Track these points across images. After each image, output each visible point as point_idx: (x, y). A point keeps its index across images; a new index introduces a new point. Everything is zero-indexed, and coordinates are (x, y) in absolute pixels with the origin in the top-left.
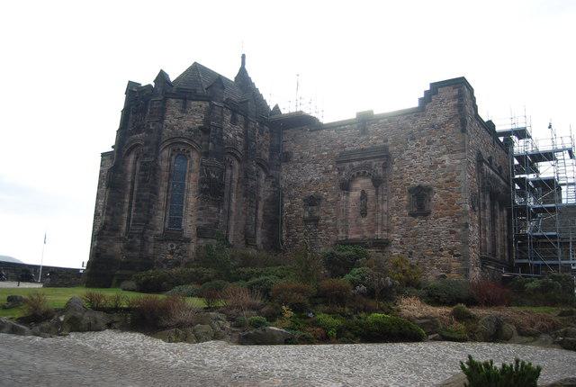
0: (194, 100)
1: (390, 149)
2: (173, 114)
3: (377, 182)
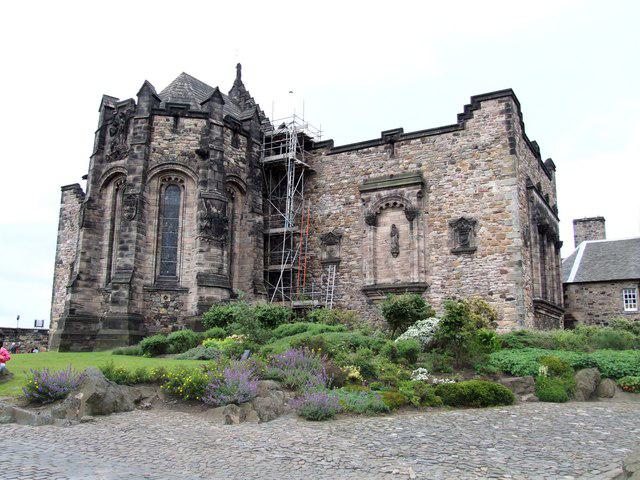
0: (187, 117)
1: (425, 175)
2: (162, 134)
3: (411, 215)
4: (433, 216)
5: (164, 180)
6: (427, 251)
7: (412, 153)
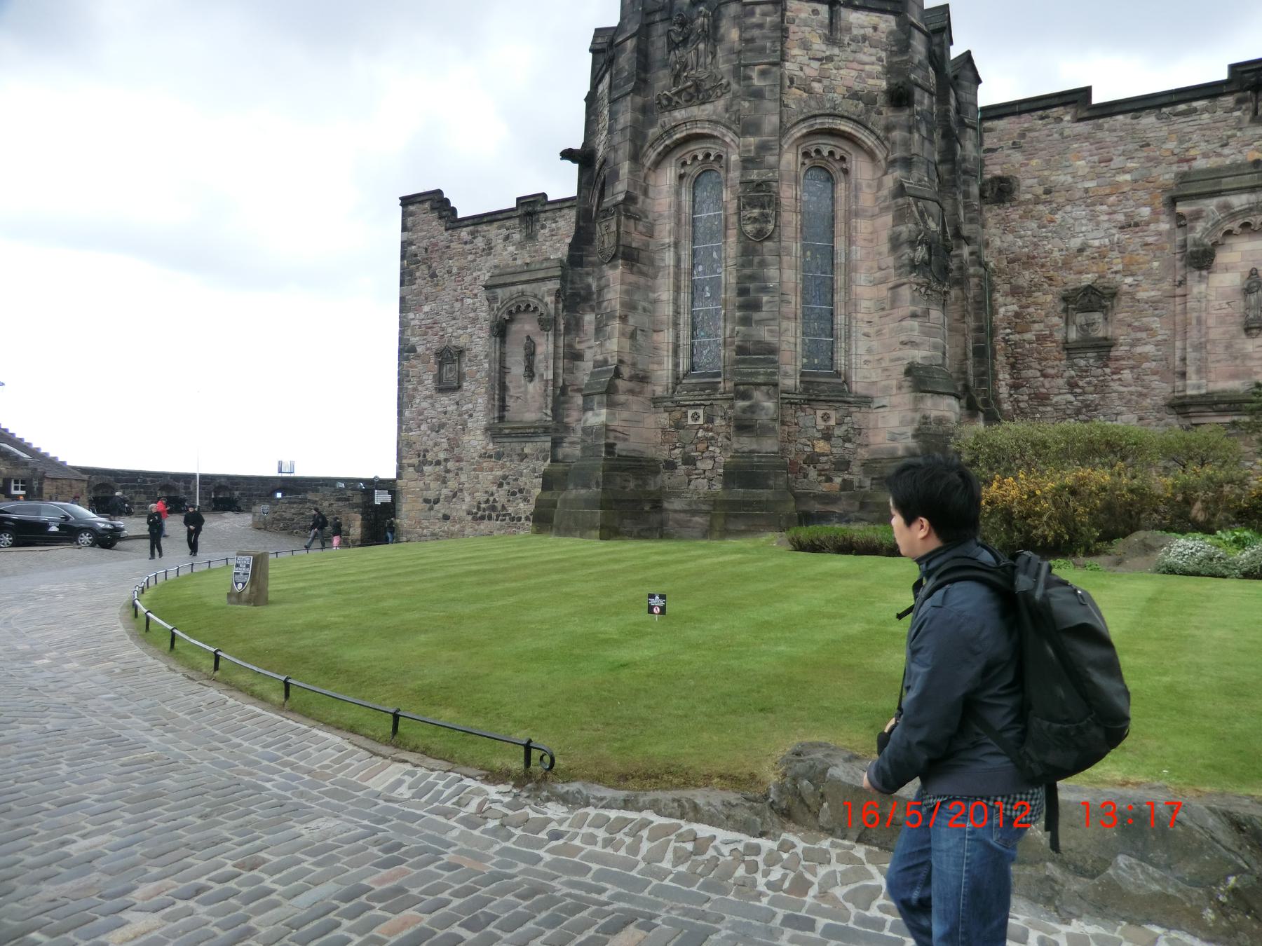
2: (806, 46)
5: (806, 154)
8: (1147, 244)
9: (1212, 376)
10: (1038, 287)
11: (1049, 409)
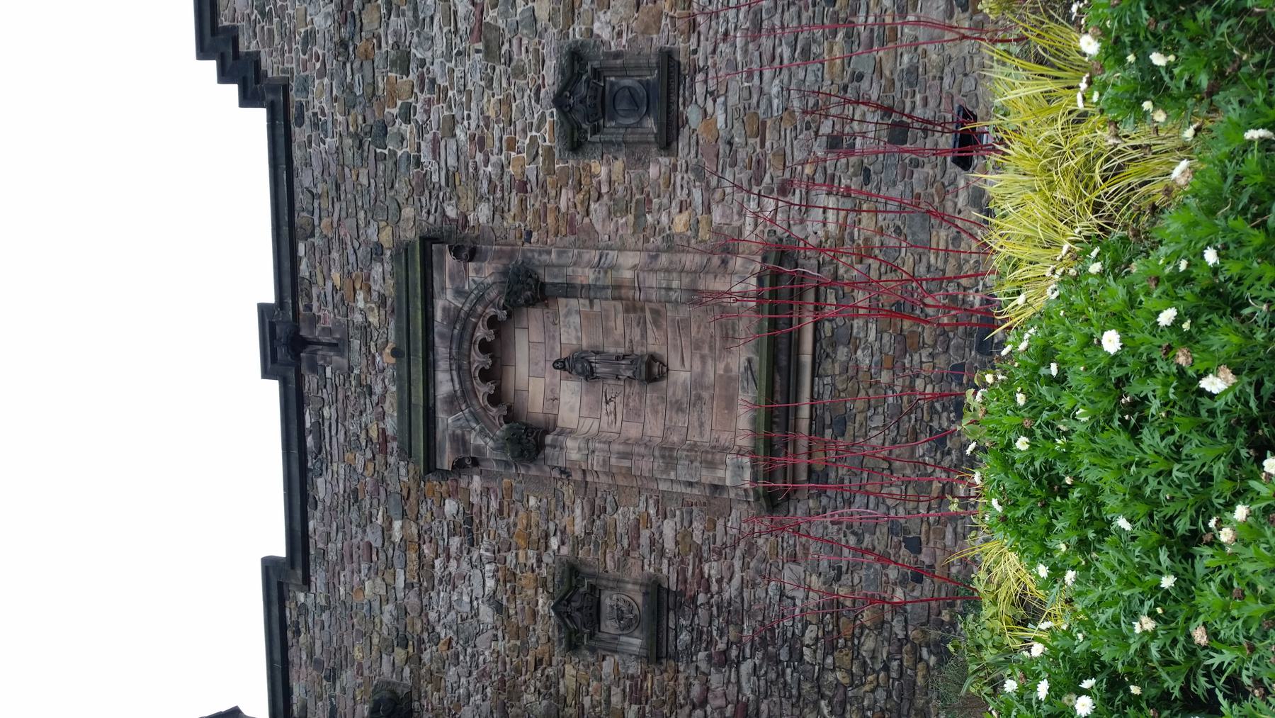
1: (410, 234)
4: (541, 215)
6: (657, 241)
7: (336, 275)
8: (501, 511)
9: (725, 438)
10: (550, 684)
11: (764, 707)
